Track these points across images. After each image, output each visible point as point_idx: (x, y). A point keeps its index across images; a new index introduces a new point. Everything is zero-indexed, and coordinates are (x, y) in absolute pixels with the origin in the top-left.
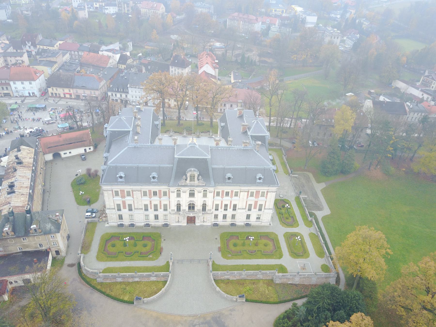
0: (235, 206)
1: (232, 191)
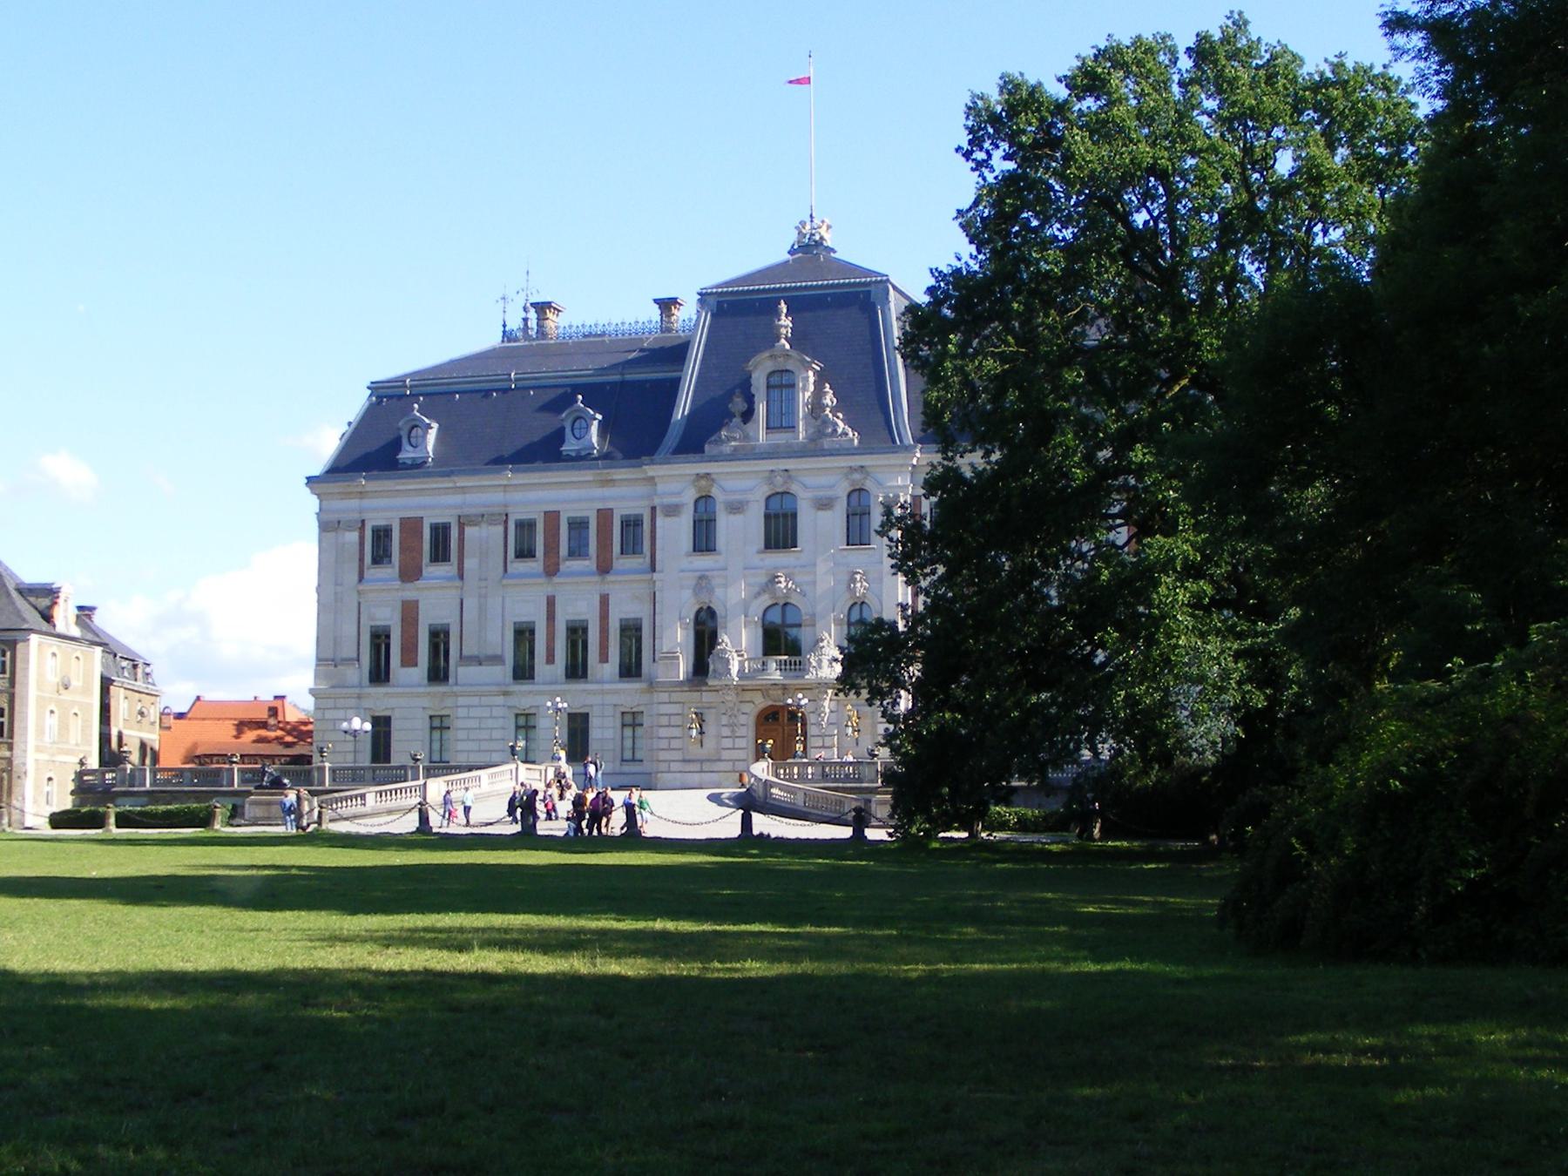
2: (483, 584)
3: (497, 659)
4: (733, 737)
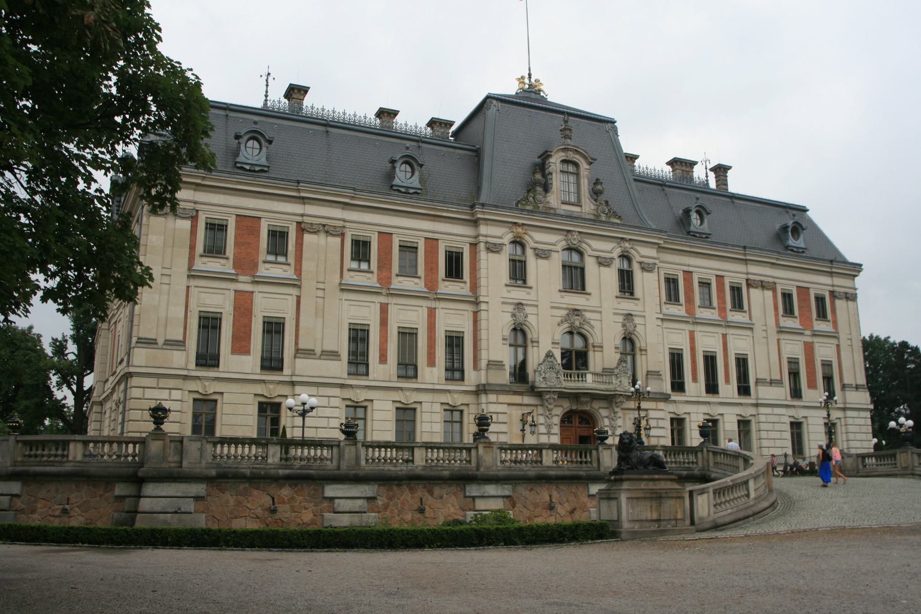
0: (742, 363)
1: (720, 278)
2: (321, 286)
3: (334, 355)
4: (549, 433)
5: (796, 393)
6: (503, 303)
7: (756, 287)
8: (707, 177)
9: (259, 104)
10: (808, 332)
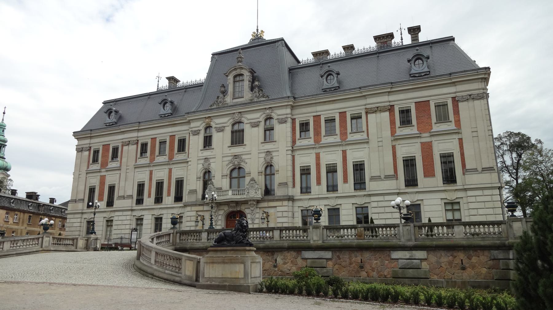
0: (359, 168)
1: (343, 115)
5: (411, 182)
6: (198, 160)
7: (373, 113)
8: (402, 39)
9: (154, 90)
10: (427, 135)
